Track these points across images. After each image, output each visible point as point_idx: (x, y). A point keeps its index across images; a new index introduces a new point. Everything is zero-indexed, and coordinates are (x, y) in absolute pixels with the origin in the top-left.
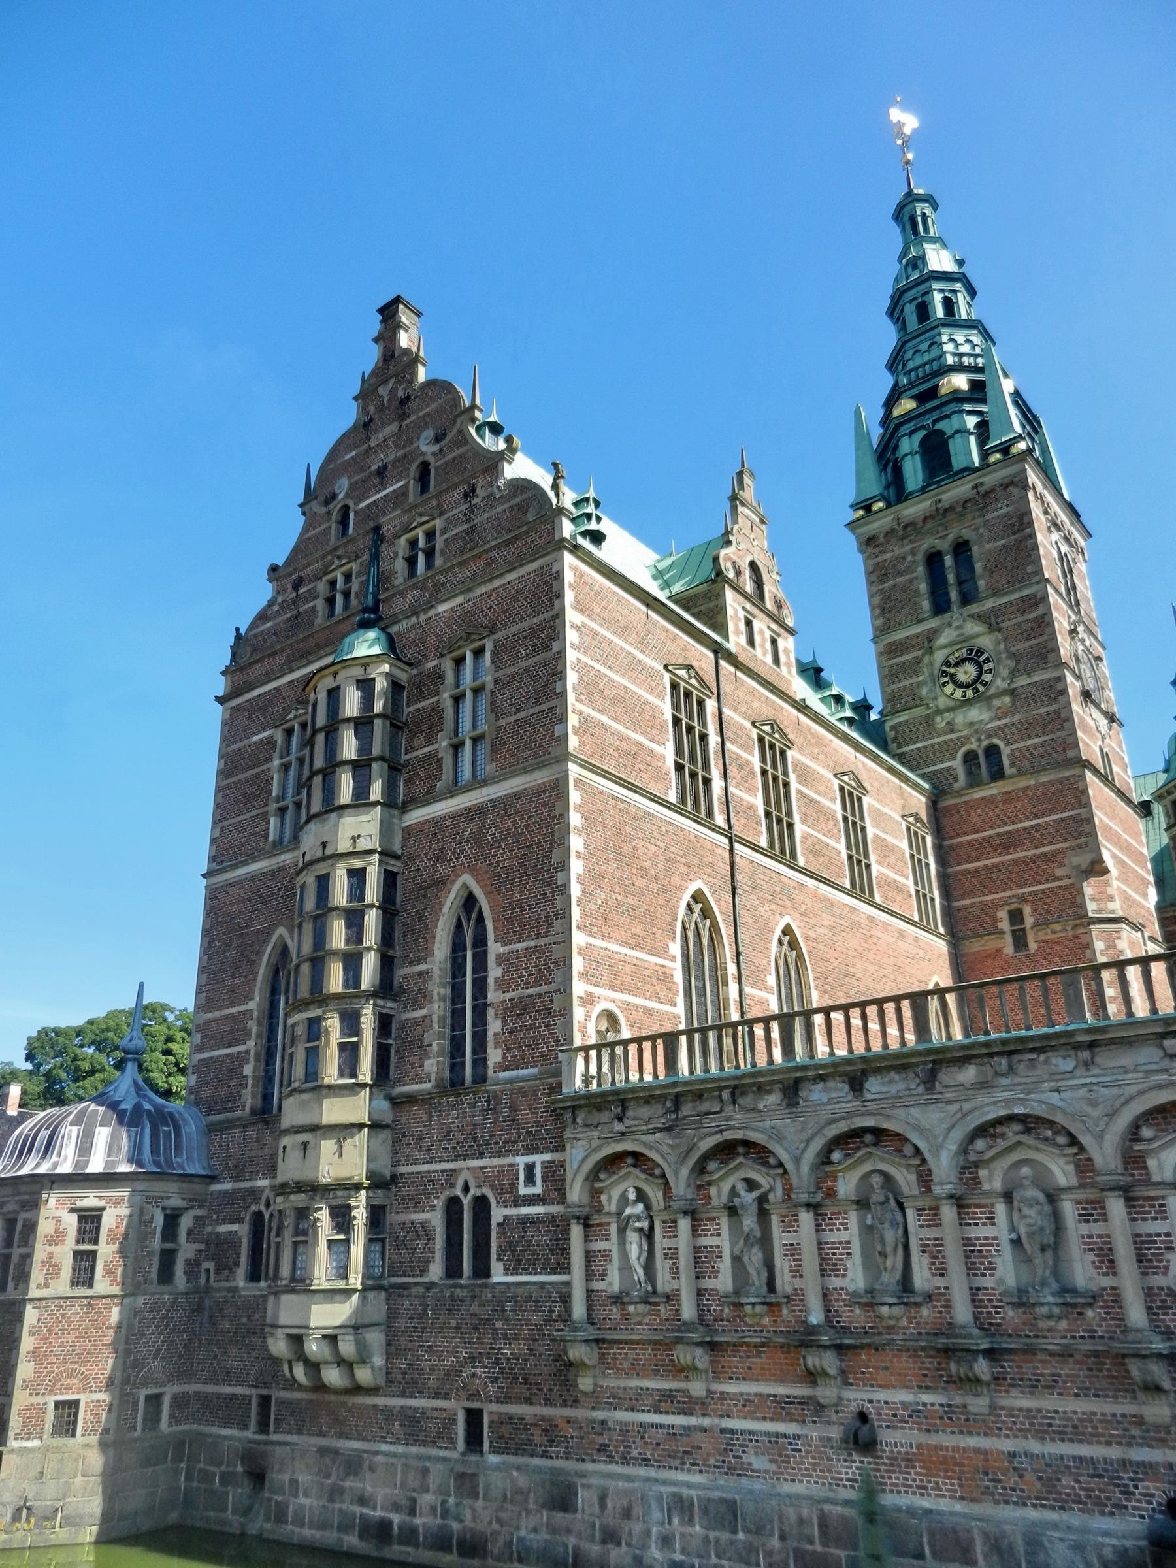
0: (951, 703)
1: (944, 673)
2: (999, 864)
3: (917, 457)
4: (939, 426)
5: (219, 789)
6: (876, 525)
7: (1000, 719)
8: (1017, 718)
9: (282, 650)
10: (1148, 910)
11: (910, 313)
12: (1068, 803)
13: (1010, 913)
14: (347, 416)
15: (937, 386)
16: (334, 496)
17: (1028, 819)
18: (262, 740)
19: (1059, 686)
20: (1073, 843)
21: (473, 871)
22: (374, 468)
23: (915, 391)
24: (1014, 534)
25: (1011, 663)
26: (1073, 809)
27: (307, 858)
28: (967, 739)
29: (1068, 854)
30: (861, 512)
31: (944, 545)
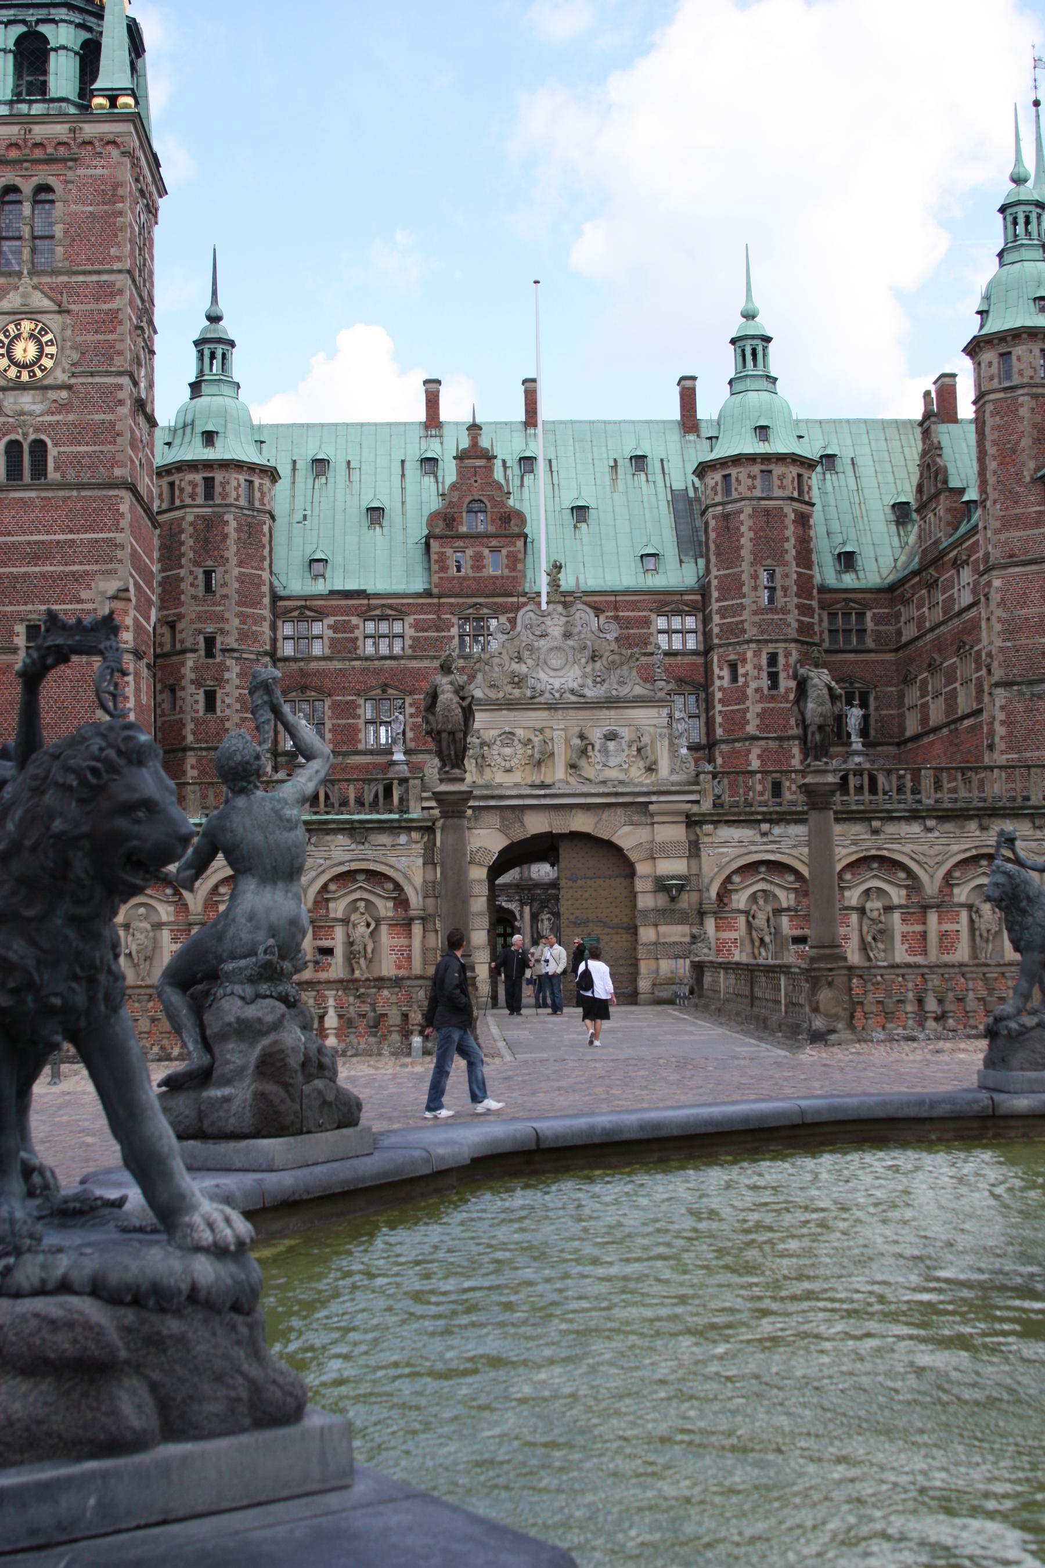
2: (25, 573)
3: (11, 56)
4: (43, 29)
7: (53, 413)
8: (71, 417)
10: (146, 632)
12: (105, 524)
13: (28, 627)
17: (63, 532)
19: (121, 395)
20: (103, 568)
24: (104, 203)
25: (76, 356)
26: (110, 531)
28: (14, 428)
29: (96, 578)
31: (27, 187)
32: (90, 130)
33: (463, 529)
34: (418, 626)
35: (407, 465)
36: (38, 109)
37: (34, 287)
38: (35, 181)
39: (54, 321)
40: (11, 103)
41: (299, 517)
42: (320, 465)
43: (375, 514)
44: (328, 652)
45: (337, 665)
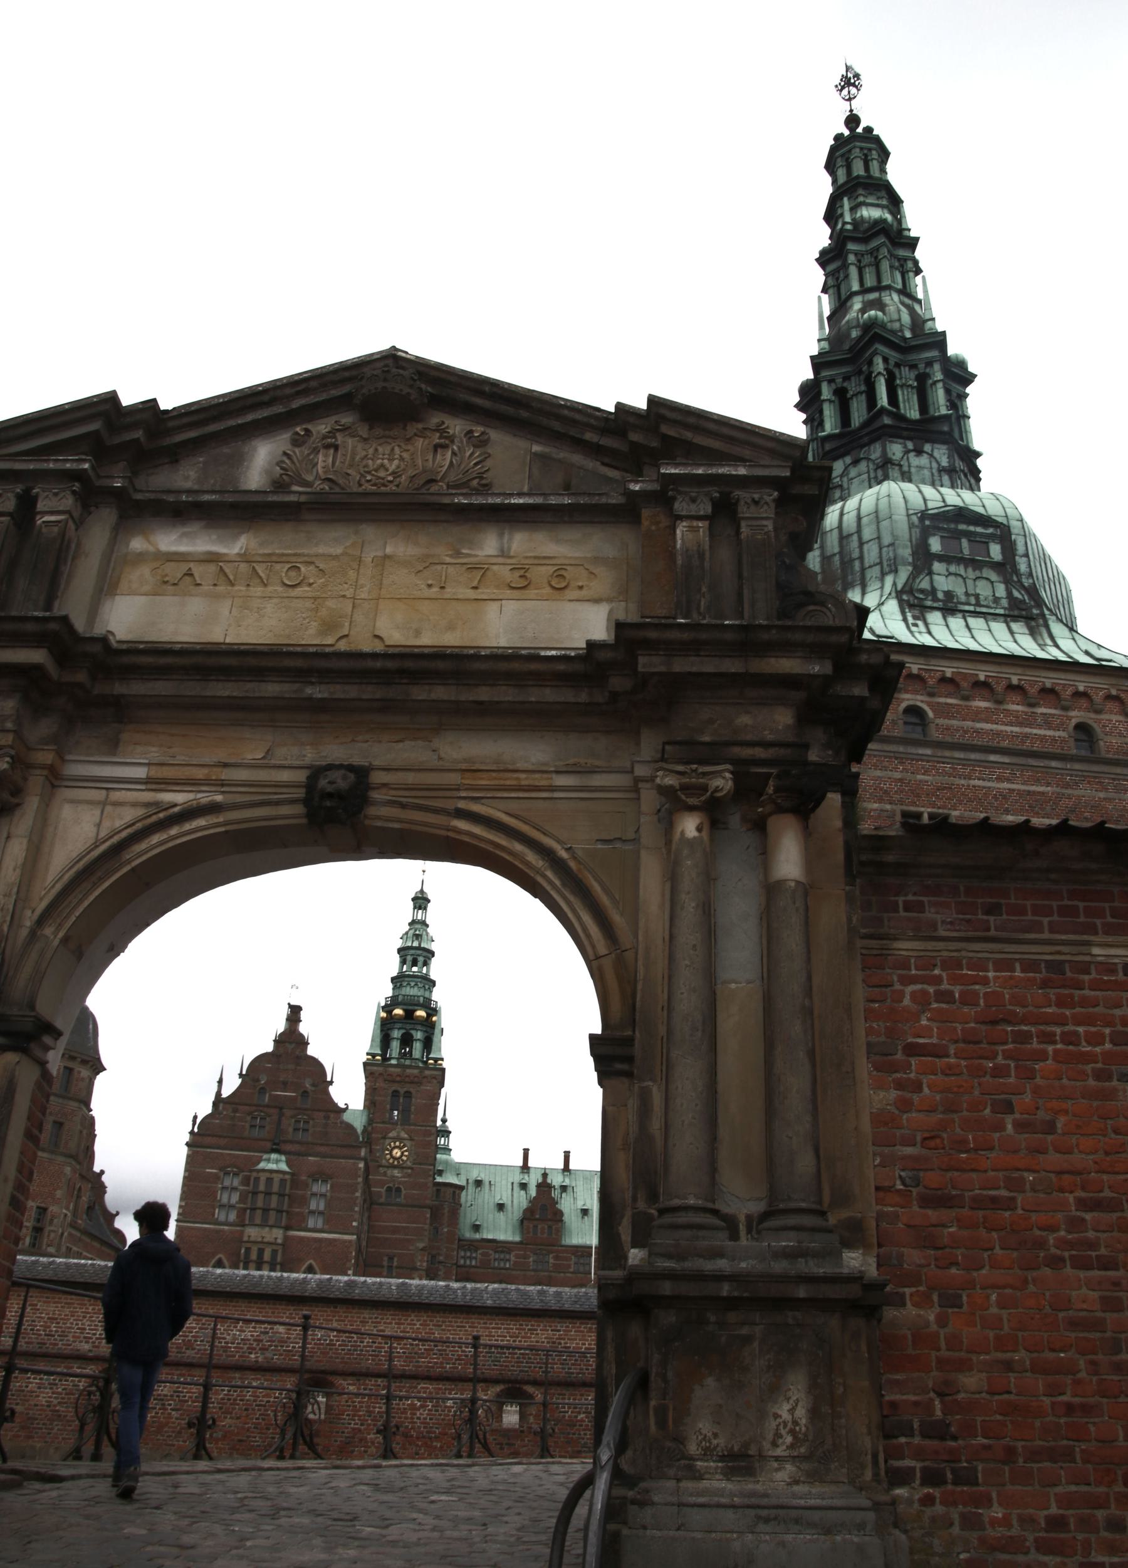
0: (387, 1164)
1: (388, 1150)
4: (413, 1032)
5: (184, 1185)
6: (375, 1068)
9: (225, 1137)
11: (409, 958)
14: (269, 1047)
15: (416, 1010)
16: (258, 1080)
18: (211, 1173)
21: (315, 1260)
22: (281, 1079)
23: (405, 1007)
27: (252, 1239)
30: (370, 1057)
31: (402, 1091)
32: (427, 1073)
33: (537, 1216)
34: (517, 1256)
35: (515, 1185)
36: (408, 1062)
37: (403, 1129)
38: (405, 1089)
39: (408, 1143)
40: (398, 1059)
41: (469, 1204)
42: (479, 1183)
43: (501, 1207)
44: (478, 1264)
45: (482, 1270)
